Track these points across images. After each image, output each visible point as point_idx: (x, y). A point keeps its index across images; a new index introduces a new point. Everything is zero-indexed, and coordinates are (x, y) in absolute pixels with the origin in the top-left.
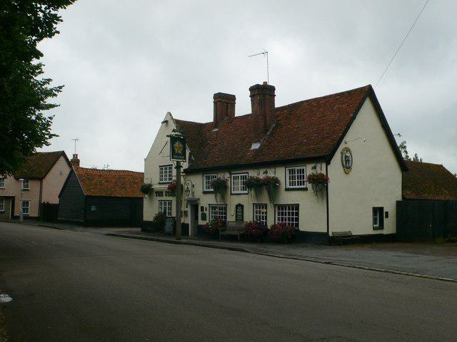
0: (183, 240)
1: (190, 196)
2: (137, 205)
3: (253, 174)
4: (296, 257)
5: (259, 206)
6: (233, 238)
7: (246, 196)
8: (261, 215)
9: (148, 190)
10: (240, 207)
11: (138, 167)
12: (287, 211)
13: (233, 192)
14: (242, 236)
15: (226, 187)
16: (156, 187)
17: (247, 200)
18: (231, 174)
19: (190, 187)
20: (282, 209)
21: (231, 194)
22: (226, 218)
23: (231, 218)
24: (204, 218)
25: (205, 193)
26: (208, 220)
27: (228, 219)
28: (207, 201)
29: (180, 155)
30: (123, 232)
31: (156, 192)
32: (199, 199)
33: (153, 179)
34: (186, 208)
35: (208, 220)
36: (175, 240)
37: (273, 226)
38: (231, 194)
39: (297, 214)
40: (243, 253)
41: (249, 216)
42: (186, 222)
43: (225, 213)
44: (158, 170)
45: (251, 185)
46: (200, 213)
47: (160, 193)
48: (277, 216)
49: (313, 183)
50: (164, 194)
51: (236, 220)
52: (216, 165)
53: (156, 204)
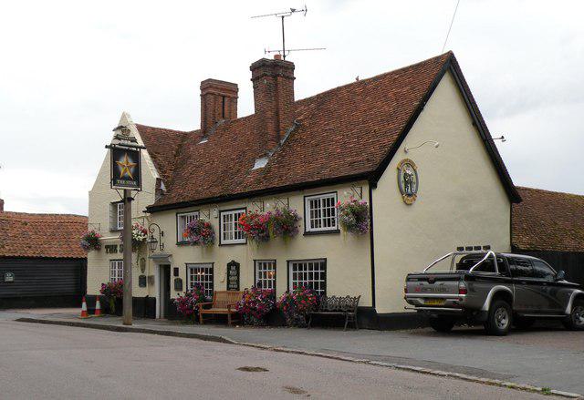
0: (135, 326)
1: (157, 251)
2: (80, 267)
3: (253, 208)
4: (335, 355)
5: (266, 265)
6: (220, 320)
7: (242, 247)
8: (268, 279)
9: (93, 242)
10: (234, 267)
11: (82, 209)
12: (308, 271)
13: (223, 242)
14: (234, 316)
15: (211, 234)
16: (108, 237)
17: (245, 254)
18: (220, 212)
19: (156, 235)
20: (301, 269)
21: (220, 245)
22: (212, 285)
23: (220, 284)
24: (179, 287)
25: (180, 244)
26: (184, 290)
27: (216, 288)
28: (184, 258)
29: (129, 179)
30: (51, 315)
31: (107, 247)
32: (171, 256)
33: (103, 226)
34: (153, 271)
35: (184, 290)
36: (121, 325)
37: (288, 297)
38: (220, 245)
39: (324, 276)
40: (222, 344)
41: (247, 282)
42: (152, 295)
43: (212, 278)
44: (108, 208)
45: (259, 232)
46: (173, 278)
47: (111, 249)
48: (291, 281)
49: (265, 168)
50: (118, 249)
51: (228, 289)
52: (201, 197)
53: (106, 266)
